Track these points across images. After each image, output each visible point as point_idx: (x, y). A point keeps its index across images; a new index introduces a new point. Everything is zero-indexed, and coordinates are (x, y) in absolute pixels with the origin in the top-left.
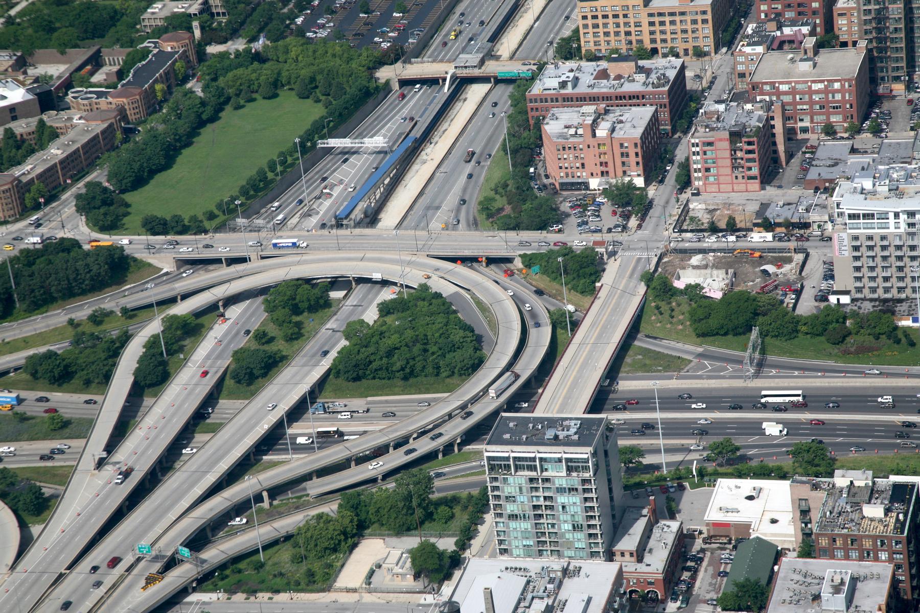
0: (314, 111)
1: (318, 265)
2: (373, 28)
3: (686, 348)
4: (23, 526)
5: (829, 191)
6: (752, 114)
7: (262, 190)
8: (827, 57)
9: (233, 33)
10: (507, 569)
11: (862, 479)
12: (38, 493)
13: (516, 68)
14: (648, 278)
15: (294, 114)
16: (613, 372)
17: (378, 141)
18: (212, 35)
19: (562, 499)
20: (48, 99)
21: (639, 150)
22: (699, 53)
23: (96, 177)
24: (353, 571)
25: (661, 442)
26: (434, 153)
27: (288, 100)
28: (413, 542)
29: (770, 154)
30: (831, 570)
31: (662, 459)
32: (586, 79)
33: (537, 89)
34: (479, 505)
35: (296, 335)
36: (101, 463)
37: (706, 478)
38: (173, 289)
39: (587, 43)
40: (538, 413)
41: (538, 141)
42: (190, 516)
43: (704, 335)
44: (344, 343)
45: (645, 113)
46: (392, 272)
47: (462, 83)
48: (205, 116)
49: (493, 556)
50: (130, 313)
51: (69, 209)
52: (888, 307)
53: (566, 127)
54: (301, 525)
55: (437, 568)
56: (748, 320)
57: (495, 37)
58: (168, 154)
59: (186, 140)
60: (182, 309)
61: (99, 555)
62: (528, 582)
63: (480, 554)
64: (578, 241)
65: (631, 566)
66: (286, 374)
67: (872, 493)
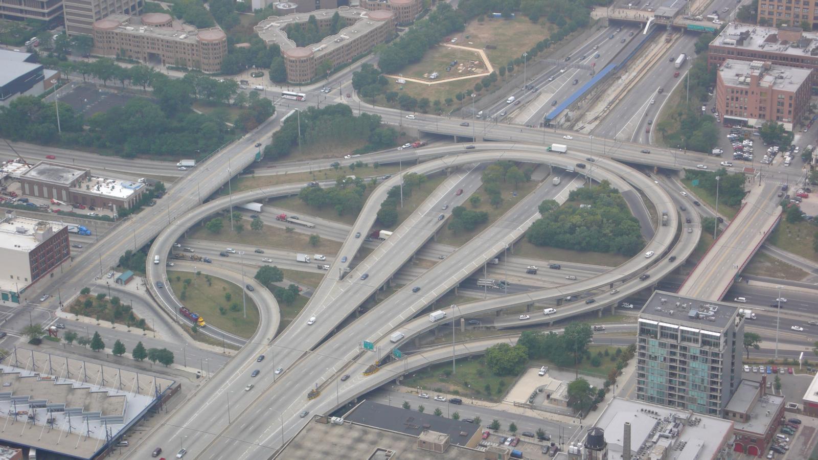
10: (642, 410)
16: (745, 273)
19: (693, 364)
21: (792, 102)
23: (370, 60)
25: (777, 333)
28: (570, 377)
33: (717, 42)
38: (415, 153)
42: (405, 327)
44: (538, 216)
49: (631, 398)
51: (348, 83)
53: (737, 75)
54: (489, 347)
60: (419, 170)
62: (658, 424)
63: (622, 395)
64: (734, 168)
66: (490, 232)
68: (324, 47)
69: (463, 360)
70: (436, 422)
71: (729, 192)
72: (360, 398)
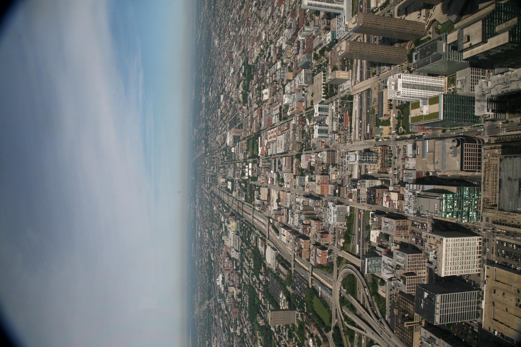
0: (315, 297)
1: (338, 298)
2: (304, 288)
3: (351, 244)
4: (375, 344)
5: (330, 225)
6: (319, 235)
7: (326, 305)
8: (312, 225)
9: (304, 308)
11: (371, 221)
12: (370, 342)
13: (311, 267)
14: (341, 250)
15: (315, 300)
16: (355, 255)
17: (320, 288)
18: (304, 311)
20: (311, 336)
22: (310, 242)
24: (383, 295)
26: (322, 280)
27: (313, 301)
28: (379, 286)
29: (324, 233)
30: (383, 225)
31: (367, 249)
32: (313, 258)
33: (314, 265)
34: (373, 275)
35: (348, 302)
36: (366, 332)
37: (370, 242)
39: (308, 257)
40: (360, 266)
41: (321, 265)
43: (349, 242)
45: (318, 249)
46: (339, 287)
47: (312, 276)
48: (315, 313)
50: (343, 327)
52: (346, 217)
55: (383, 282)
56: (348, 236)
57: (306, 270)
58: (320, 319)
59: (318, 316)
60: (343, 319)
61: (379, 333)
64: (335, 259)
65: (383, 253)
66: (353, 303)
67: (372, 220)
68: (321, 339)
69: (379, 307)
70: (392, 311)
71: (340, 259)
72: (389, 327)
